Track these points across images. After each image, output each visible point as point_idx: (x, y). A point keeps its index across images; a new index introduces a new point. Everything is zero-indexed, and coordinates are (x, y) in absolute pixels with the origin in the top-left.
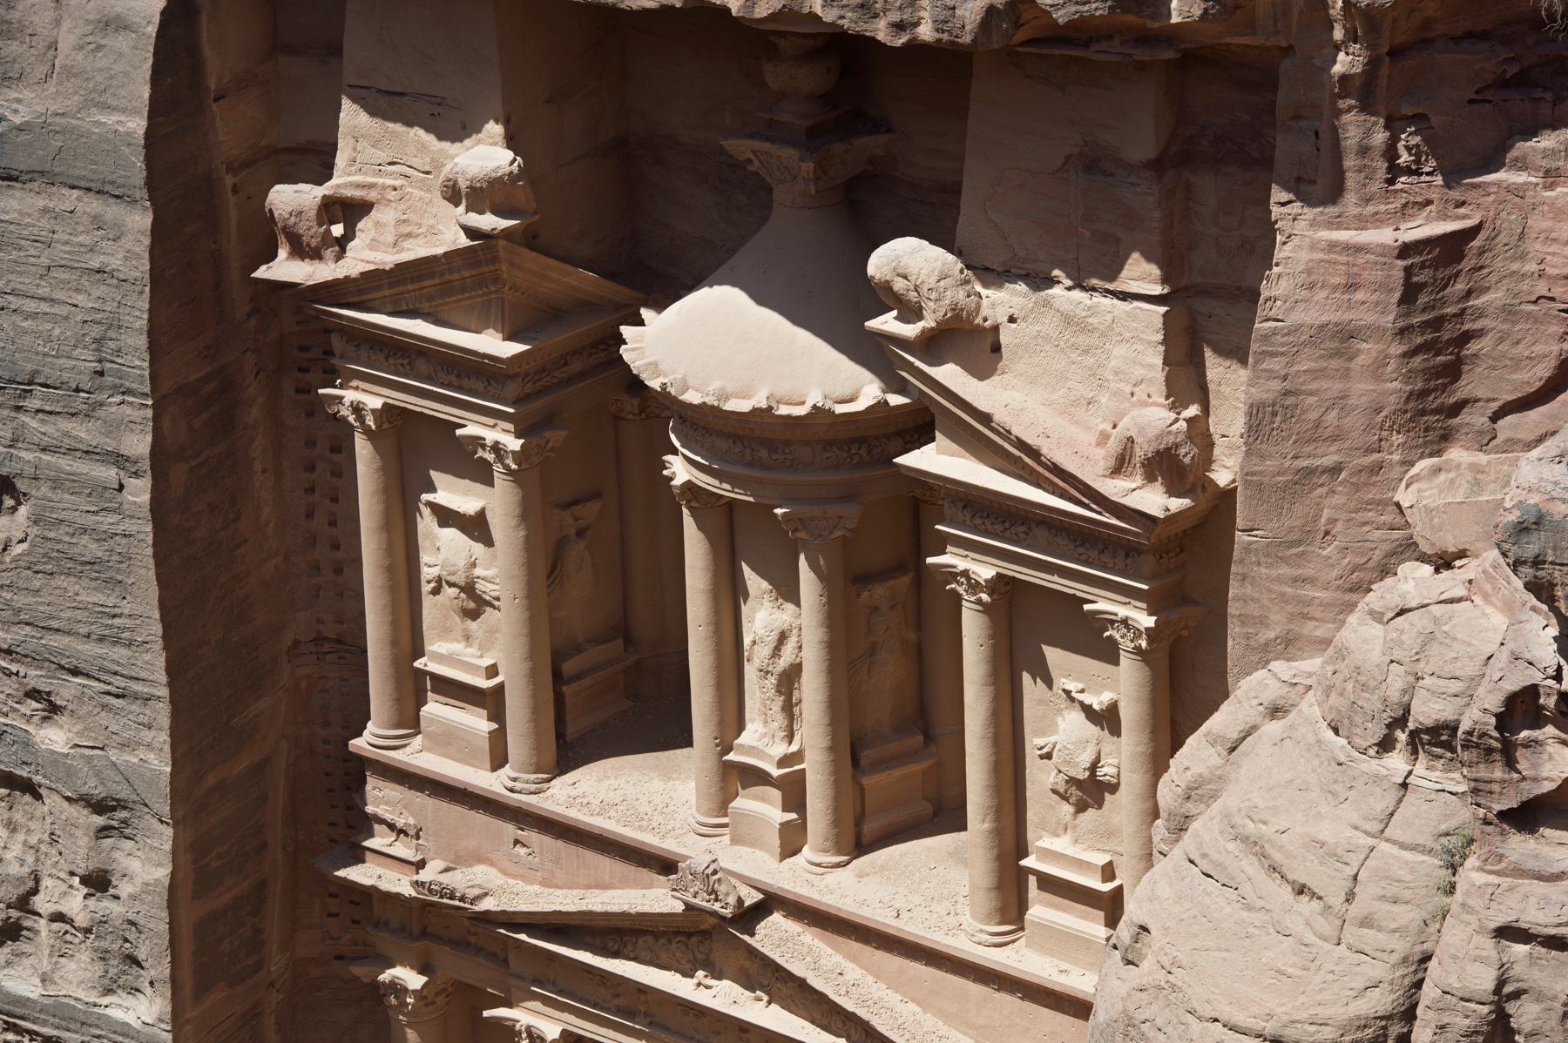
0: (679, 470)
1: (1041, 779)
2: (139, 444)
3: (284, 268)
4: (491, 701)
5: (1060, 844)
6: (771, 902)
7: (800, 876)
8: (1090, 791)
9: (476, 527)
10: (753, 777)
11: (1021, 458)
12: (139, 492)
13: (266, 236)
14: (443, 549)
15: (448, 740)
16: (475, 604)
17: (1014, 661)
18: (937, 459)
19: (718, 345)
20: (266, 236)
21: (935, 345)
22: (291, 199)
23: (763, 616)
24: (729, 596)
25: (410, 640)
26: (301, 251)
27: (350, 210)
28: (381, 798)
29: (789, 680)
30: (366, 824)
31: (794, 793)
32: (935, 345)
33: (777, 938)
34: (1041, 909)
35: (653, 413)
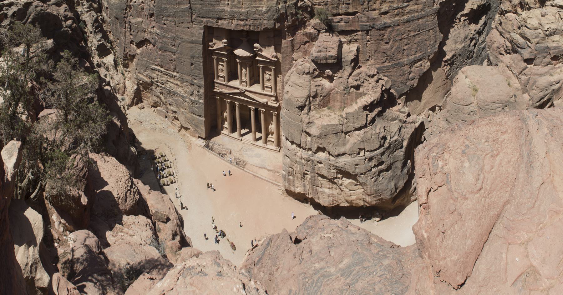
0: (238, 60)
1: (265, 79)
2: (202, 61)
3: (210, 48)
4: (224, 77)
5: (267, 84)
6: (246, 90)
7: (247, 88)
8: (269, 80)
9: (223, 65)
10: (244, 82)
11: (266, 58)
12: (202, 64)
13: (209, 46)
14: (220, 67)
15: (221, 80)
16: (222, 70)
17: (264, 72)
18: (258, 58)
19: (240, 52)
20: (209, 46)
21: (258, 51)
22: (210, 44)
23: (244, 70)
24: (241, 70)
25: (218, 73)
26: (212, 47)
27: (214, 44)
28: (216, 85)
29: (246, 75)
30: (215, 86)
31: (246, 82)
32: (258, 51)
33: (247, 93)
34: (266, 89)
35: (236, 57)
